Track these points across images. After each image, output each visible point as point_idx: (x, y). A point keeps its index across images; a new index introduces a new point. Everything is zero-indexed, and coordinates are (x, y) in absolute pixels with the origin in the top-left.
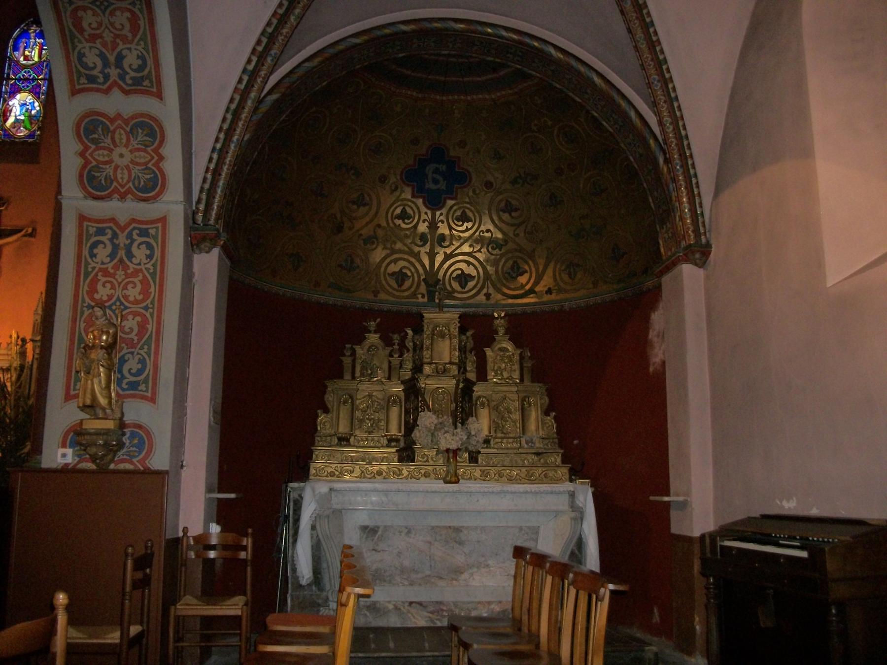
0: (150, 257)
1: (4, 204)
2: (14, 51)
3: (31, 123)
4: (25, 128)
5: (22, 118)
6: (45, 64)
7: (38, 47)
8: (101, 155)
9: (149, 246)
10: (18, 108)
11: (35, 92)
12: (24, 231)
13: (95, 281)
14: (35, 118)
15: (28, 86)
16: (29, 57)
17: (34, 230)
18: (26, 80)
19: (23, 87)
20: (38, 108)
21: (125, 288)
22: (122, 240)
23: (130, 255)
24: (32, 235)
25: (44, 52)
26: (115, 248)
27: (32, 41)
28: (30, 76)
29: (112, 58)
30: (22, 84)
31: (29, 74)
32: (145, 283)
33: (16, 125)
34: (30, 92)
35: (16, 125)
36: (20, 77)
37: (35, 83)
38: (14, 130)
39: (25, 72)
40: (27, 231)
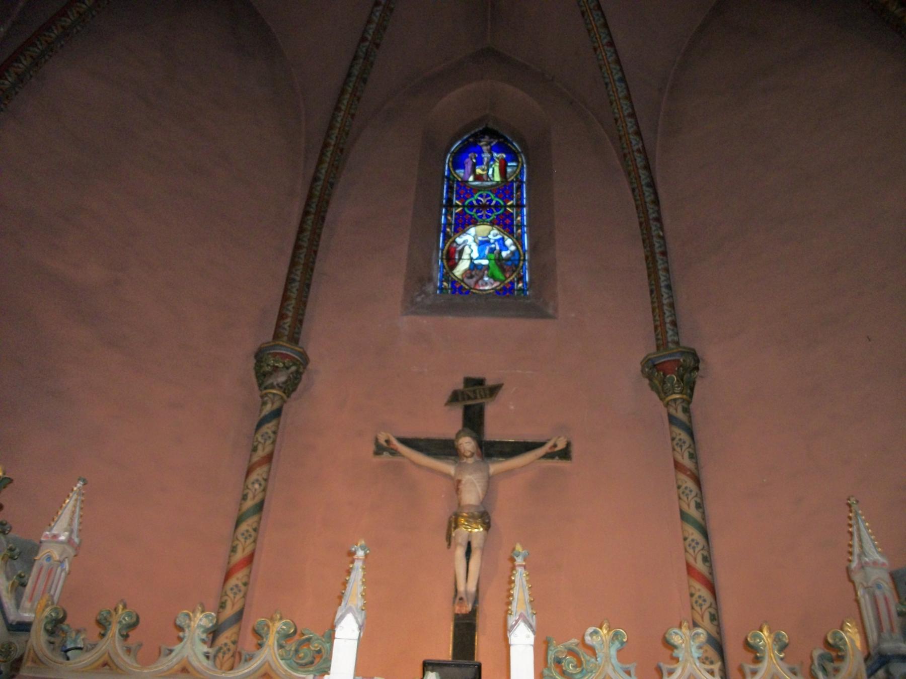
2: (455, 169)
3: (503, 271)
4: (492, 277)
5: (485, 262)
6: (515, 185)
7: (497, 164)
10: (475, 247)
11: (505, 223)
12: (550, 444)
14: (509, 263)
15: (488, 217)
16: (485, 177)
18: (480, 207)
19: (481, 217)
20: (513, 248)
24: (565, 454)
25: (509, 170)
27: (486, 156)
28: (491, 201)
30: (477, 212)
31: (489, 198)
33: (473, 273)
34: (492, 224)
35: (473, 273)
36: (471, 203)
37: (501, 212)
38: (471, 282)
39: (481, 196)
40: (555, 446)
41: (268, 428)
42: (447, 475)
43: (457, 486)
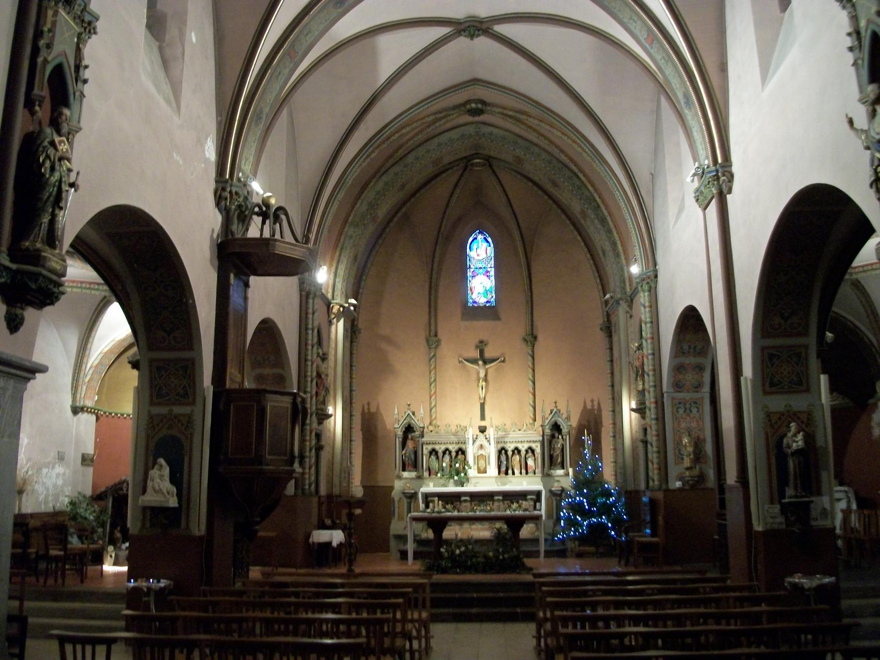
0: (698, 411)
1: (486, 344)
8: (681, 377)
9: (697, 407)
13: (679, 421)
17: (504, 359)
18: (481, 268)
21: (691, 423)
22: (688, 406)
23: (691, 411)
24: (503, 361)
26: (685, 409)
29: (692, 347)
32: (697, 421)
41: (433, 360)
42: (476, 369)
43: (478, 373)
